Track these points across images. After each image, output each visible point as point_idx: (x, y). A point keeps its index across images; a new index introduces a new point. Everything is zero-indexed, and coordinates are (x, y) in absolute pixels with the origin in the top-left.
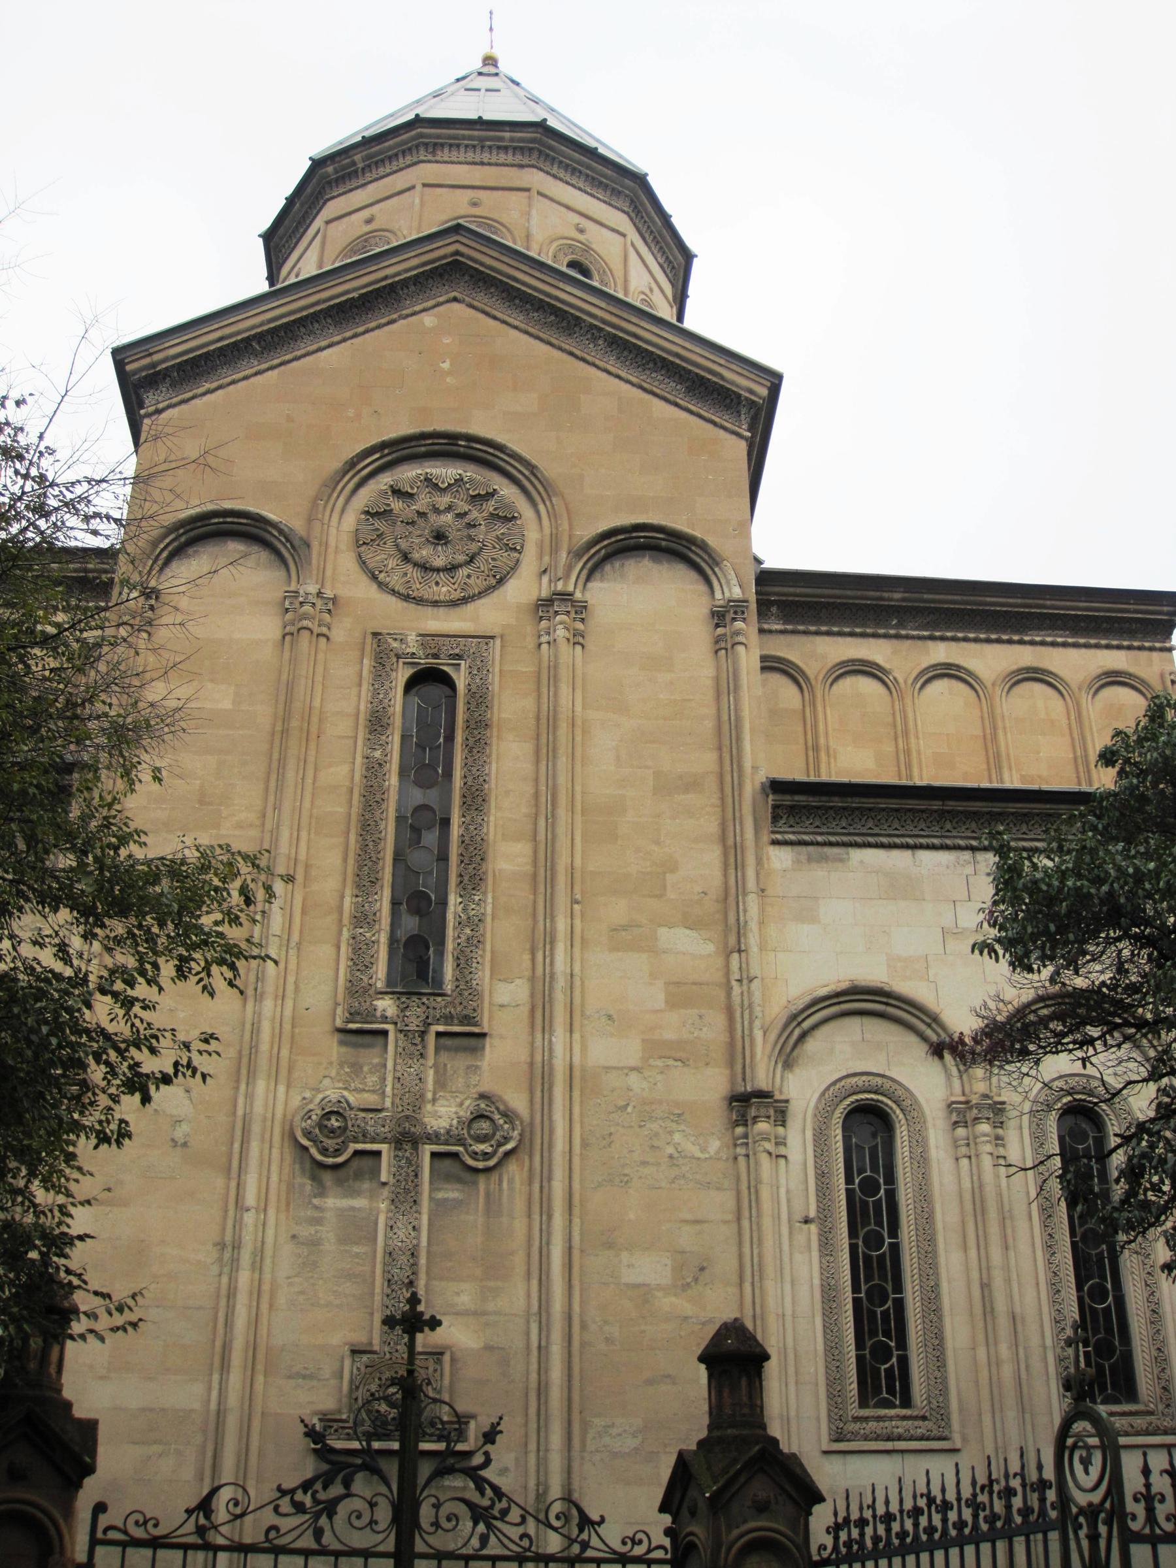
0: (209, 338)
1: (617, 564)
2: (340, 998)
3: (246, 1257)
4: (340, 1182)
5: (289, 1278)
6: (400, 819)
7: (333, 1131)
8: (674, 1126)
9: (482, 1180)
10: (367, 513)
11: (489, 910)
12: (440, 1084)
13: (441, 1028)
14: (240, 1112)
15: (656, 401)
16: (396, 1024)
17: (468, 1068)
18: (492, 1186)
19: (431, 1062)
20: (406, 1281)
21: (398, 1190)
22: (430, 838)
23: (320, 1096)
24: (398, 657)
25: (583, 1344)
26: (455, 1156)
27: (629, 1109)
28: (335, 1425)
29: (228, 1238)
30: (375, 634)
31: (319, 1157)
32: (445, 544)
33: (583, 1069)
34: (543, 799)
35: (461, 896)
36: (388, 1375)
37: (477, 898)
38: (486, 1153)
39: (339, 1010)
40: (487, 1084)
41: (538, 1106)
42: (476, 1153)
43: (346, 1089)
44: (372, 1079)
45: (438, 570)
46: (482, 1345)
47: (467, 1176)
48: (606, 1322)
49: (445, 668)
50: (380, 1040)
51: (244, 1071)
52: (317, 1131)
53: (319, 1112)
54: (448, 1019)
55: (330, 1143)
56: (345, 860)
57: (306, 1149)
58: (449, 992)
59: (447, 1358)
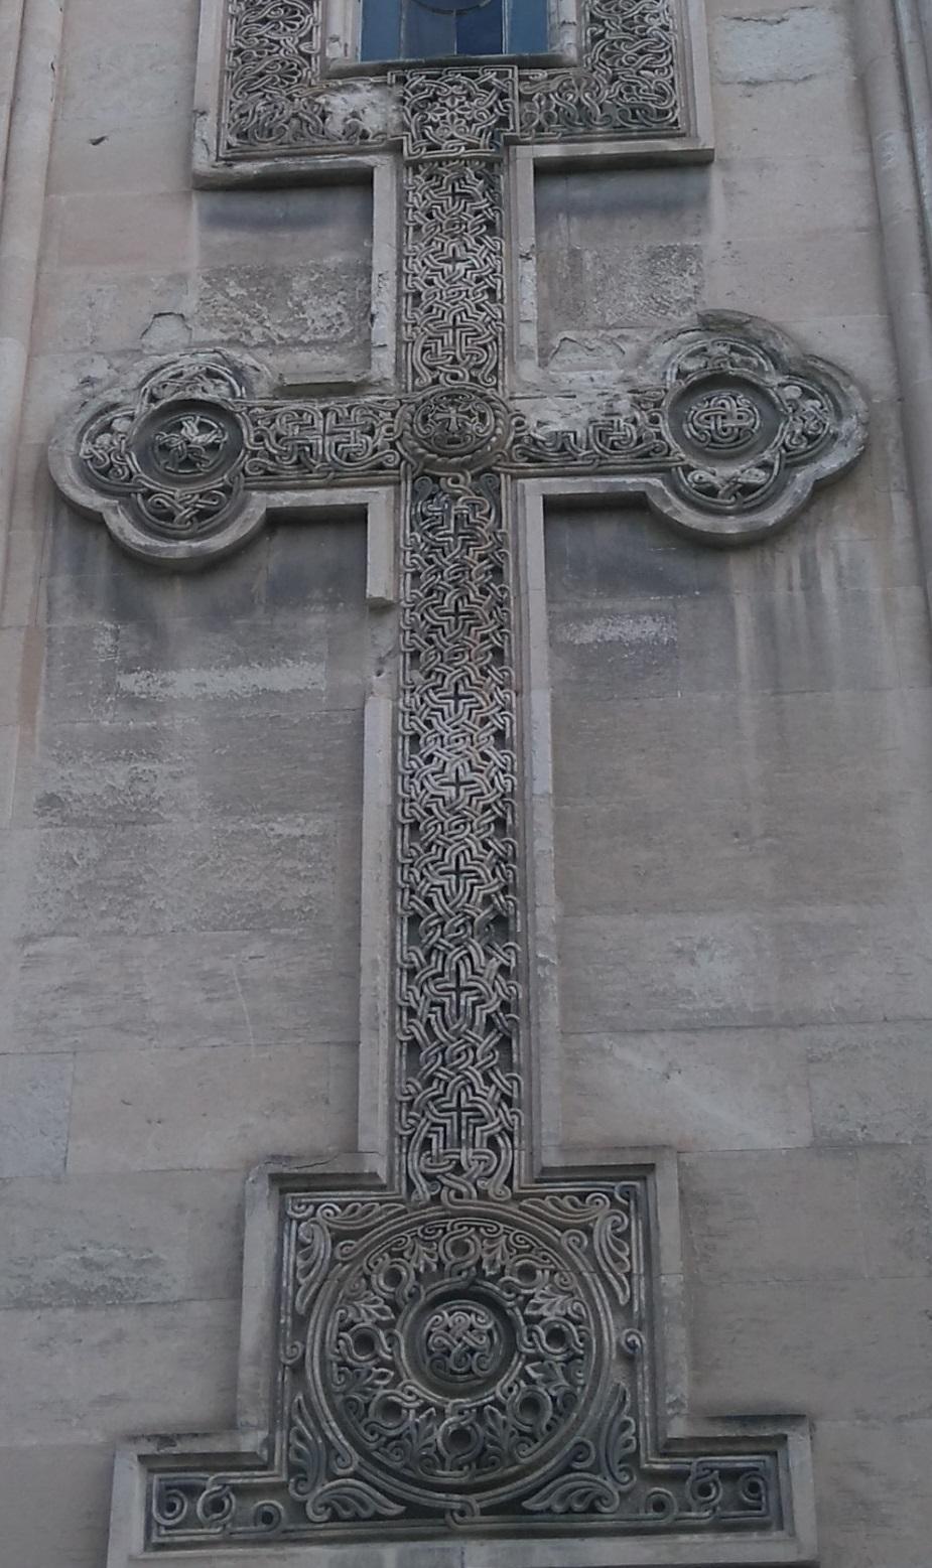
2: (207, 92)
4: (217, 618)
5: (29, 939)
9: (739, 572)
16: (396, 148)
18: (780, 592)
19: (526, 241)
20: (483, 914)
23: (143, 367)
26: (635, 505)
28: (211, 1483)
31: (136, 538)
36: (421, 1259)
38: (748, 489)
39: (206, 129)
40: (723, 293)
42: (712, 491)
44: (321, 312)
46: (803, 1136)
50: (345, 203)
52: (133, 462)
53: (141, 408)
54: (576, 122)
55: (180, 497)
57: (92, 520)
59: (666, 1185)
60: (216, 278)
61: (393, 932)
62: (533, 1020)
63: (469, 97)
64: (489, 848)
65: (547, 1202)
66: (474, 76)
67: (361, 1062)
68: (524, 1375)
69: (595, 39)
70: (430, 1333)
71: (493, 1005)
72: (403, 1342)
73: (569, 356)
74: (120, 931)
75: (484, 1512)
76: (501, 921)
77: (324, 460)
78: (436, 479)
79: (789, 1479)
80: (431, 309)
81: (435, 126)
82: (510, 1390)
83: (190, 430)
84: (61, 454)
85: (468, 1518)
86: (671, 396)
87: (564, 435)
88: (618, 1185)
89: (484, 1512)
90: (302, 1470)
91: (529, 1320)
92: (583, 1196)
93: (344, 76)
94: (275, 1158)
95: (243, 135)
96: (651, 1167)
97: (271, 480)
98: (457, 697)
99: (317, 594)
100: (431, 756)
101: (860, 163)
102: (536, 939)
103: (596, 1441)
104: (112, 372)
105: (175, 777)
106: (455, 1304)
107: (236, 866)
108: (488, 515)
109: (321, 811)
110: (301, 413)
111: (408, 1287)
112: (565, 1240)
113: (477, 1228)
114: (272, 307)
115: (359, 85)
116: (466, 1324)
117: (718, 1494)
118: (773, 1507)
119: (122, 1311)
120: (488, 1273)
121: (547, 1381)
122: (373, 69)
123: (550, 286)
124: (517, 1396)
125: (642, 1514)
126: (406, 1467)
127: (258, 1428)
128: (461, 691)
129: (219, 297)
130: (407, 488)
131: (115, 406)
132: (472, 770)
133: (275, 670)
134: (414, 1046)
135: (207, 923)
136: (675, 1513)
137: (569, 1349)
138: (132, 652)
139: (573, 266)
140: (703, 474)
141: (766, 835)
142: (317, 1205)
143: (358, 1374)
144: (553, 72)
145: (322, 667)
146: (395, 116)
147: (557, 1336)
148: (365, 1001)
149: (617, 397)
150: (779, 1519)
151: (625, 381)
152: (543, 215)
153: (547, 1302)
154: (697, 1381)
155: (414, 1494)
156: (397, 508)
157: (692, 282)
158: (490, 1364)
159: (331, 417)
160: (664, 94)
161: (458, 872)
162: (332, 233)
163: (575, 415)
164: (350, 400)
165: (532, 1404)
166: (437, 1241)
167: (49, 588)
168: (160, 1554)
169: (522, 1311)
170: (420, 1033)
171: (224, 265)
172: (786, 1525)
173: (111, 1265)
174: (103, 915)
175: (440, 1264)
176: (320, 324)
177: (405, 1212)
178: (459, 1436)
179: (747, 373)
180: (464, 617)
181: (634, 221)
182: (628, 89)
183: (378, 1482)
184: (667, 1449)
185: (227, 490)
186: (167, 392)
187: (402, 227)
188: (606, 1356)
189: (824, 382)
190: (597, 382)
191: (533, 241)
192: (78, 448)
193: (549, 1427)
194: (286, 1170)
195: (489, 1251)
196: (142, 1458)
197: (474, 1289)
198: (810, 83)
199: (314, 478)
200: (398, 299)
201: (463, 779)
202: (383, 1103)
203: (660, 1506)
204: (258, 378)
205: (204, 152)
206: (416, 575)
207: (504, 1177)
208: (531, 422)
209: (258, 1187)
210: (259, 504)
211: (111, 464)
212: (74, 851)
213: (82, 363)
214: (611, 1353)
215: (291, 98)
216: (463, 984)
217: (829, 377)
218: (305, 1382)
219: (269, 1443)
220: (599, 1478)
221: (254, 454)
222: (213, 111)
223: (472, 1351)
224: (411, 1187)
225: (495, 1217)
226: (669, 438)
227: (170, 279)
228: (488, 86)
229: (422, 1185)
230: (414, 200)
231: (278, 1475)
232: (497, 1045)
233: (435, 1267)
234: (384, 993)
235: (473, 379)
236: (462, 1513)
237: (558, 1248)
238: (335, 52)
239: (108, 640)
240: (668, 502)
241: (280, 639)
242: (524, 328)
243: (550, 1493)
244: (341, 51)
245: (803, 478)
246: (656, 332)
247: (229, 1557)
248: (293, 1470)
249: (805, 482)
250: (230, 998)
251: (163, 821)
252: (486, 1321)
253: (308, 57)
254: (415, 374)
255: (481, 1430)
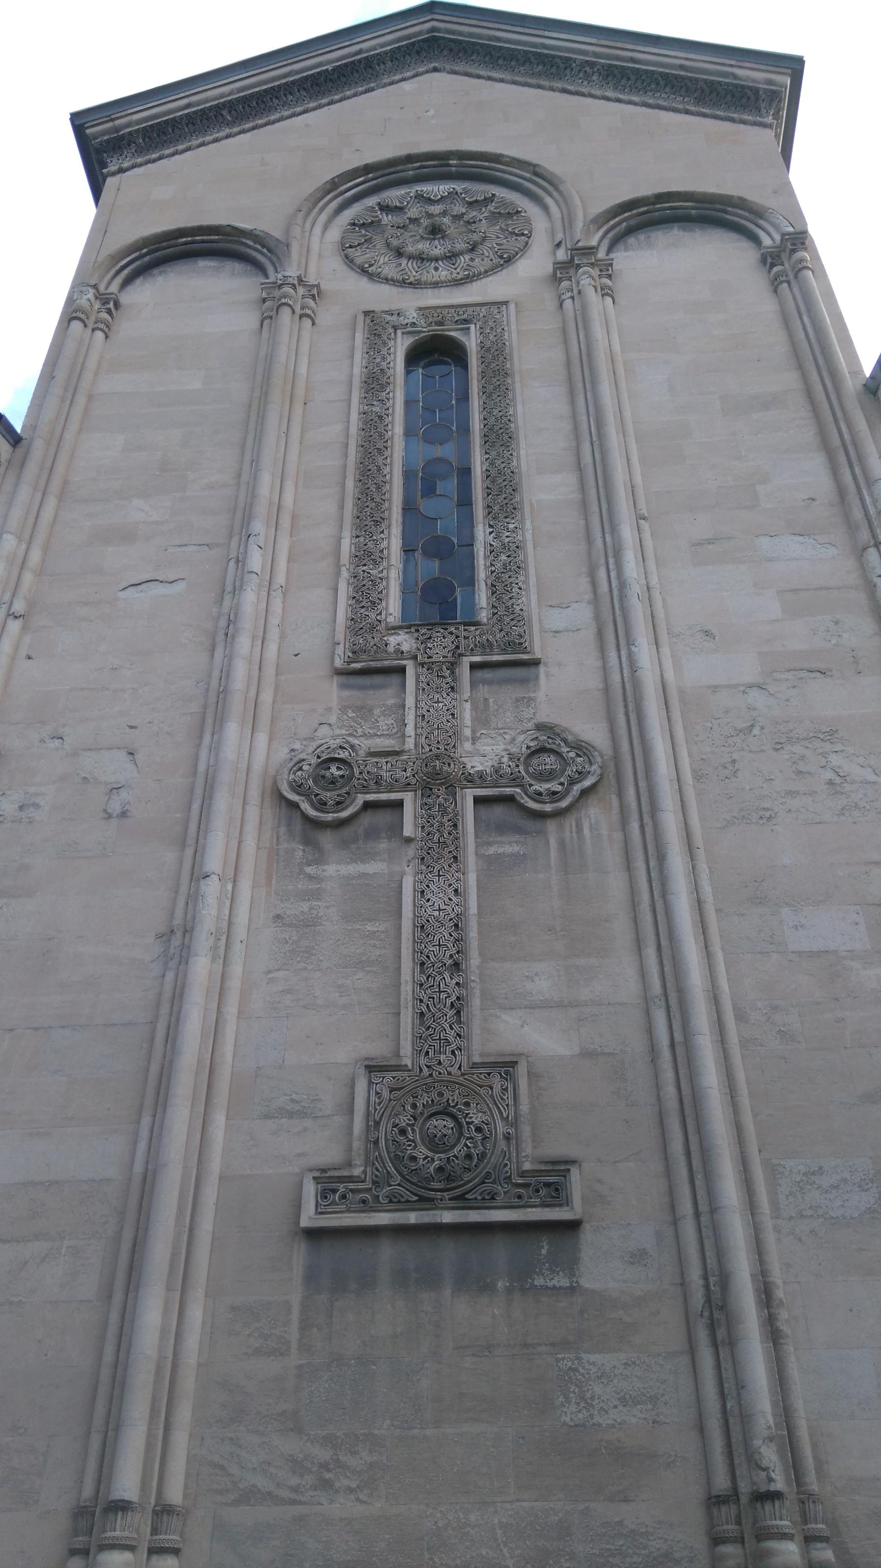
0: (174, 106)
1: (642, 237)
2: (340, 636)
3: (203, 942)
4: (344, 844)
5: (269, 972)
6: (408, 475)
7: (333, 781)
8: (827, 747)
9: (551, 826)
10: (354, 224)
11: (529, 536)
12: (482, 719)
13: (477, 659)
14: (202, 768)
15: (662, 113)
16: (415, 658)
17: (517, 700)
18: (567, 834)
19: (467, 694)
21: (430, 844)
22: (449, 486)
23: (314, 745)
24: (395, 328)
25: (744, 1043)
26: (509, 800)
27: (756, 731)
28: (341, 1188)
29: (178, 921)
30: (367, 313)
31: (312, 812)
32: (443, 238)
33: (681, 692)
34: (585, 426)
35: (490, 526)
36: (425, 1099)
37: (511, 526)
38: (554, 793)
39: (340, 650)
40: (545, 715)
41: (623, 731)
42: (540, 794)
43: (350, 735)
44: (385, 723)
45: (437, 260)
46: (577, 1050)
47: (530, 824)
48: (775, 1008)
49: (452, 334)
50: (395, 679)
51: (209, 721)
52: (310, 782)
53: (314, 761)
54: (486, 647)
55: (329, 796)
56: (342, 507)
57: (295, 805)
58: (485, 620)
59: (522, 1069)
60: (343, 709)
61: (414, 969)
62: (469, 1004)
63: (444, 637)
64: (452, 936)
65: (475, 1076)
66: (446, 629)
67: (401, 1020)
68: (466, 1145)
69: (494, 614)
70: (428, 1128)
71: (454, 998)
72: (418, 1132)
73: (484, 740)
74: (305, 969)
75: (450, 1199)
76: (456, 965)
77: (386, 781)
78: (431, 789)
79: (571, 1186)
80: (429, 721)
81: (430, 649)
82: (460, 1151)
83: (333, 770)
84: (282, 779)
85: (443, 1202)
86: (524, 756)
87: (482, 772)
88: (503, 1070)
89: (450, 1199)
90: (377, 1182)
91: (468, 1123)
92: (489, 1074)
93: (394, 629)
94: (367, 1059)
95: (354, 652)
96: (516, 1063)
97: (365, 790)
98: (439, 876)
99: (383, 835)
100: (429, 899)
101: (599, 663)
102: (470, 972)
103: (494, 1171)
104: (302, 747)
105: (327, 907)
106: (438, 1117)
107: (351, 943)
108: (452, 803)
109: (385, 921)
110: (377, 763)
111: (420, 1110)
112: (482, 1091)
113: (447, 1087)
114: (366, 721)
115: (400, 632)
116: (442, 1125)
117: (543, 1192)
118: (564, 1197)
119: (306, 1119)
120: (452, 1104)
121: (475, 1147)
122: (406, 626)
123: (476, 712)
124: (463, 1153)
125: (512, 1200)
126: (419, 1181)
127: (360, 1166)
128: (441, 873)
129: (345, 717)
130: (419, 792)
131: (303, 760)
132: (445, 905)
133: (367, 865)
134: (422, 1014)
135: (340, 965)
136: (526, 1200)
137: (484, 1135)
138: (310, 858)
139: (485, 705)
140: (537, 787)
141: (561, 931)
142: (384, 1078)
143: (400, 1145)
144: (477, 627)
145: (386, 864)
146: (415, 645)
147: (479, 1129)
148: (402, 997)
149: (503, 757)
150: (567, 1202)
151: (506, 750)
152: (473, 684)
153: (475, 1116)
154: (534, 1147)
155: (422, 1192)
156: (415, 800)
157: (532, 711)
158: (452, 1141)
159: (389, 765)
160: (521, 636)
161: (439, 945)
162: (390, 692)
163: (486, 764)
164: (397, 758)
165: (469, 1156)
166: (431, 1092)
167: (277, 832)
168: (322, 1216)
169: (465, 1119)
170: (424, 1009)
171: (346, 704)
172: (570, 1204)
173: (302, 1101)
174: (299, 962)
175: (432, 1101)
176: (385, 727)
177: (418, 1080)
178: (440, 1169)
179: (554, 747)
180: (442, 844)
181: (509, 686)
182: (507, 634)
183: (408, 1187)
184: (522, 1174)
185: (348, 793)
186: (324, 754)
187: (417, 689)
188: (498, 1137)
189: (585, 751)
190: (495, 751)
191: (469, 694)
192: (289, 777)
193: (476, 1166)
194: (371, 1064)
195: (452, 1096)
196: (314, 1178)
197: (446, 1111)
198: (579, 632)
199: (382, 789)
200: (416, 718)
201: (441, 908)
202: (410, 1037)
203: (520, 1197)
204: (360, 749)
205: (339, 659)
206: (423, 827)
207: (458, 1066)
208: (469, 766)
209: (360, 1070)
210: (361, 799)
211: (302, 783)
212: (287, 937)
213: (290, 743)
214: (500, 1136)
215: (373, 638)
216: (442, 990)
217: (587, 749)
218: (379, 1149)
219: (365, 1172)
220: (495, 1186)
221: (359, 779)
222: (342, 643)
223: (445, 1136)
224: (421, 1070)
225: (454, 1082)
226: (523, 773)
227: (325, 710)
228: (451, 633)
229: (425, 1069)
230: (422, 678)
231: (368, 1185)
232: (455, 1014)
233: (430, 1102)
234: (410, 993)
235: (446, 749)
236: (441, 1200)
237: (479, 1095)
238: (391, 619)
239: (301, 853)
240: (523, 798)
241: (369, 853)
242: (466, 729)
243: (476, 1192)
244: (393, 619)
245: (577, 789)
246: (518, 731)
247: (349, 1217)
248: (374, 1183)
249: (577, 790)
250: (349, 995)
251: (323, 925)
252: (450, 1123)
253: (380, 621)
254: (423, 747)
255: (449, 1167)
